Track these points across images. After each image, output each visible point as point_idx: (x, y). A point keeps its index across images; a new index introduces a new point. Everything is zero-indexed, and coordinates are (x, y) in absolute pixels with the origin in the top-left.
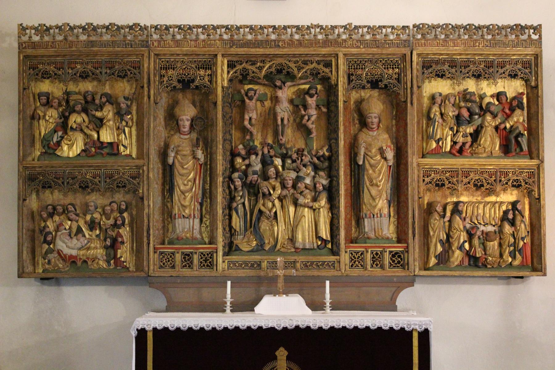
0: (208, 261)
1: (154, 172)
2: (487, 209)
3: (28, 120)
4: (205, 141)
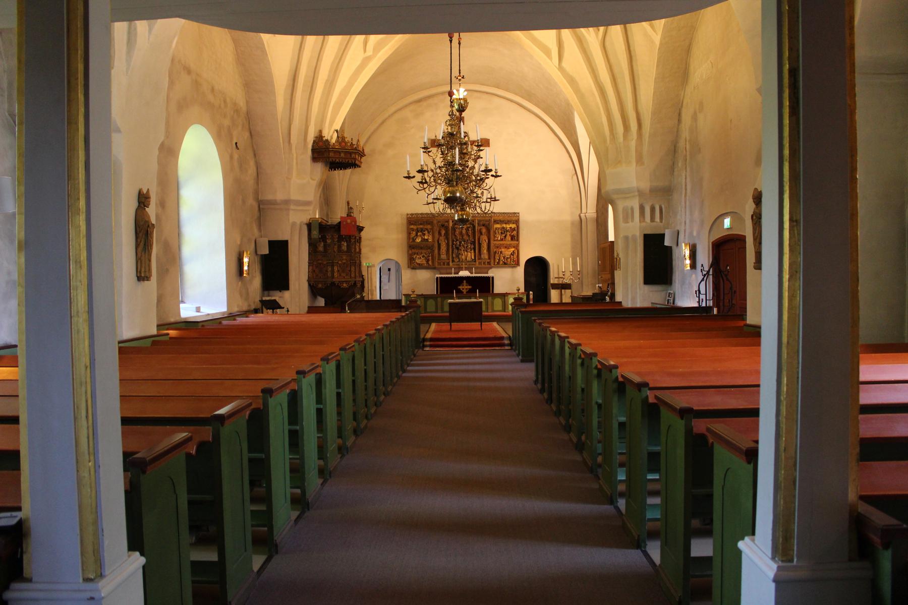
0: (448, 264)
1: (436, 245)
2: (507, 252)
3: (409, 234)
4: (447, 239)
